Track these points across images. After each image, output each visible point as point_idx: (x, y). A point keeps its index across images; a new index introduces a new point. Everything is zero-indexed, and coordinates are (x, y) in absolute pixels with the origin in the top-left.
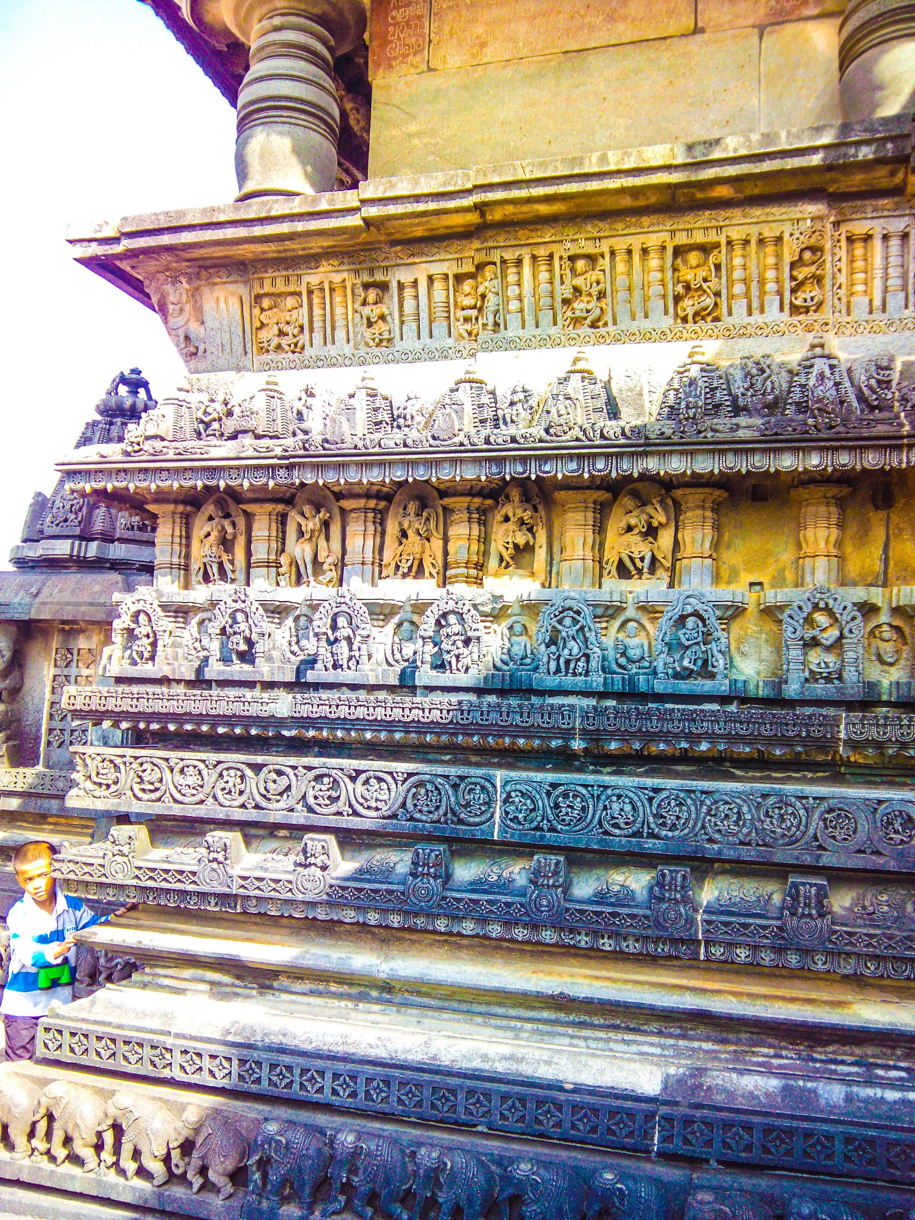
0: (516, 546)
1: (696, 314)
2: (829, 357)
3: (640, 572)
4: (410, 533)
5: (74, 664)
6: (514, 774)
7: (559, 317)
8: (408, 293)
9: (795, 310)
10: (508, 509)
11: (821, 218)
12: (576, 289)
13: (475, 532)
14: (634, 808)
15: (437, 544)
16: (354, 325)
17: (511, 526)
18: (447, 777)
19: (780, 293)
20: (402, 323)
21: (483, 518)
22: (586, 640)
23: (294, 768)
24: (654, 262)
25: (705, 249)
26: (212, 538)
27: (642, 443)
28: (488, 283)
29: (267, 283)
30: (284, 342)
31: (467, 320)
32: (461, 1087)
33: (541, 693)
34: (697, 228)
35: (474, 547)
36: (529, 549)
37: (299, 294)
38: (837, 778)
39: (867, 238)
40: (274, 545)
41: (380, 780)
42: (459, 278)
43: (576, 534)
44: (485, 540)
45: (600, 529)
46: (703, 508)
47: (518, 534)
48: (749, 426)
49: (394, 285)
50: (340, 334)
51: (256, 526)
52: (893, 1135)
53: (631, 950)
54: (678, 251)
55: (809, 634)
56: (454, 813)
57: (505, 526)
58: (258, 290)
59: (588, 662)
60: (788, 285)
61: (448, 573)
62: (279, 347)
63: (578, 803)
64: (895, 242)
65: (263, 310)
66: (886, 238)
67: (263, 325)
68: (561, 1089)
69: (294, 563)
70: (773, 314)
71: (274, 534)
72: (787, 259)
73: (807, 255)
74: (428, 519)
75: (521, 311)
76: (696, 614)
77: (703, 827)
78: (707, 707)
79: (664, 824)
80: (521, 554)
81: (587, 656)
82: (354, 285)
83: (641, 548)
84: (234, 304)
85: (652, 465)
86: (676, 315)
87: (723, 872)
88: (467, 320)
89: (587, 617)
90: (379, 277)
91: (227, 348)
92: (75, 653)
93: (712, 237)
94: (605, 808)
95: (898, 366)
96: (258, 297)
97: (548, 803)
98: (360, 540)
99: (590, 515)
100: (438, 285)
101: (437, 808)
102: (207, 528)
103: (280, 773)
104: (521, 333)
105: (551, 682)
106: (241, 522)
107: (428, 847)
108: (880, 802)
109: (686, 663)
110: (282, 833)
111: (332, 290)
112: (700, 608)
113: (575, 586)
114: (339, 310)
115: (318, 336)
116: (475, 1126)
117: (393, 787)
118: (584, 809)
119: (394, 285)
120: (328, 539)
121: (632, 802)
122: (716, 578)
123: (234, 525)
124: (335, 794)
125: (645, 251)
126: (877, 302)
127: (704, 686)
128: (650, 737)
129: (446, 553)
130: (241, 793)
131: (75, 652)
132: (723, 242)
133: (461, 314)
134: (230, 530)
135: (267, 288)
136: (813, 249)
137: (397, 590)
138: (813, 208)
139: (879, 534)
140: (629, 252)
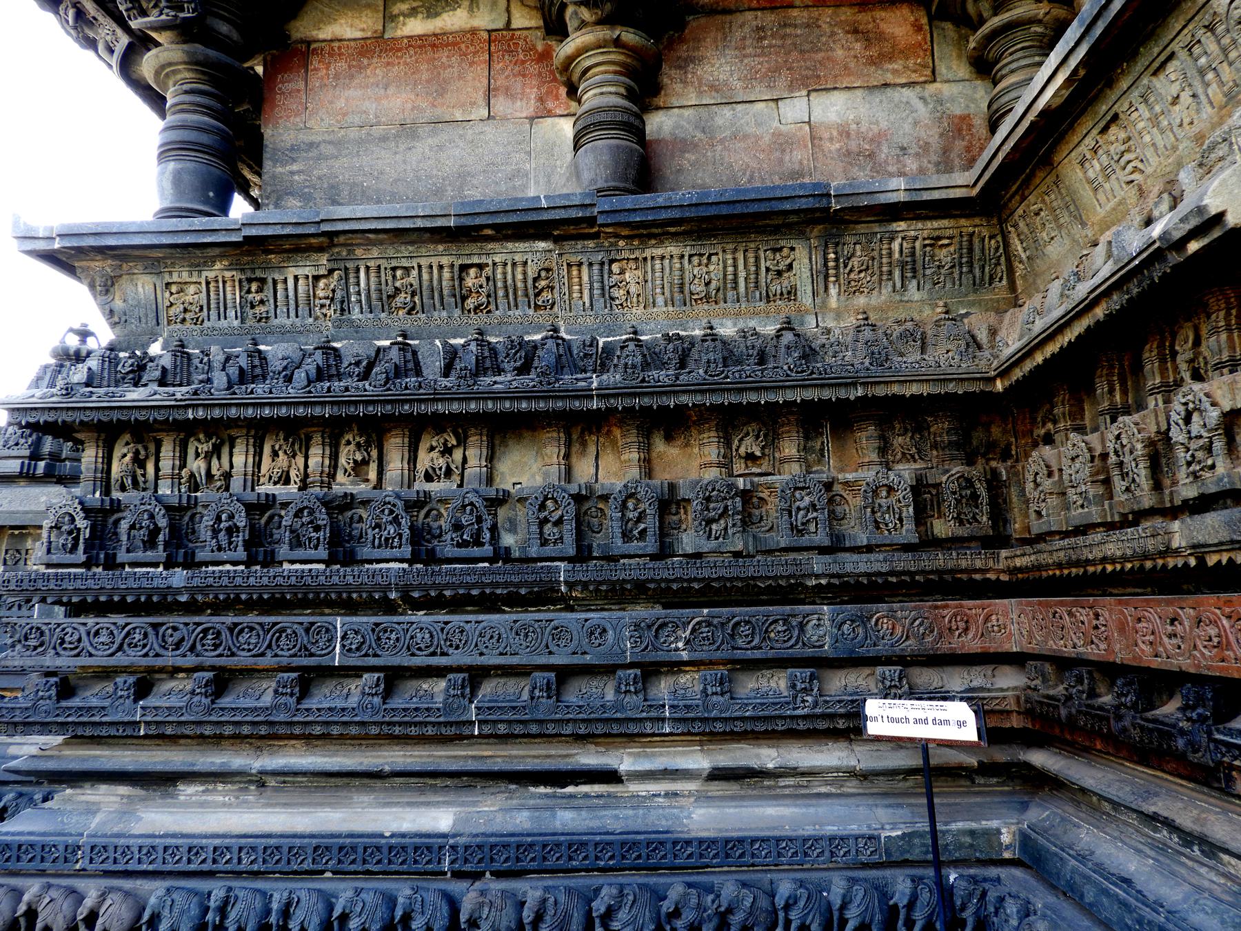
0: (355, 461)
1: (476, 308)
2: (558, 338)
3: (439, 477)
4: (280, 453)
5: (22, 562)
6: (348, 619)
7: (386, 307)
8: (280, 287)
9: (537, 307)
10: (349, 437)
11: (550, 251)
12: (396, 289)
13: (327, 452)
14: (432, 636)
15: (300, 460)
16: (241, 307)
17: (352, 447)
18: (301, 624)
19: (527, 295)
20: (276, 306)
22: (399, 524)
23: (186, 624)
24: (446, 274)
25: (481, 267)
26: (127, 459)
29: (175, 275)
30: (188, 316)
31: (322, 306)
32: (310, 844)
33: (370, 562)
35: (327, 462)
36: (365, 462)
37: (200, 283)
38: (571, 609)
39: (580, 264)
40: (177, 463)
41: (252, 629)
42: (317, 278)
44: (335, 457)
46: (481, 435)
47: (357, 454)
49: (270, 281)
50: (231, 313)
51: (163, 449)
52: (598, 838)
53: (430, 733)
54: (464, 268)
55: (542, 515)
56: (306, 649)
57: (348, 448)
58: (167, 279)
59: (400, 539)
60: (531, 292)
61: (309, 480)
62: (184, 320)
63: (393, 636)
64: (596, 268)
65: (172, 294)
66: (591, 265)
67: (172, 304)
68: (382, 836)
69: (192, 475)
71: (177, 454)
72: (531, 274)
73: (543, 274)
74: (293, 444)
75: (360, 301)
76: (472, 504)
77: (476, 645)
78: (481, 565)
79: (451, 646)
81: (400, 536)
82: (240, 281)
84: (149, 288)
85: (440, 407)
86: (463, 308)
87: (497, 676)
88: (322, 306)
89: (399, 509)
90: (259, 274)
91: (143, 320)
92: (23, 552)
93: (483, 260)
94: (412, 637)
95: (601, 344)
96: (168, 285)
97: (373, 638)
99: (406, 440)
100: (301, 282)
101: (294, 646)
102: (125, 450)
103: (175, 629)
104: (360, 316)
105: (377, 554)
106: (152, 448)
107: (286, 675)
108: (586, 620)
109: (465, 537)
110: (181, 675)
111: (224, 282)
112: (474, 500)
114: (229, 296)
115: (213, 313)
116: (322, 872)
117: (261, 633)
118: (398, 639)
119: (270, 281)
120: (219, 458)
121: (430, 632)
123: (146, 448)
124: (218, 642)
125: (441, 267)
126: (587, 304)
127: (476, 551)
128: (441, 587)
129: (306, 466)
130: (144, 646)
131: (23, 552)
132: (490, 263)
133: (317, 301)
134: (143, 452)
135: (175, 278)
136: (548, 270)
139: (592, 449)
140: (431, 267)
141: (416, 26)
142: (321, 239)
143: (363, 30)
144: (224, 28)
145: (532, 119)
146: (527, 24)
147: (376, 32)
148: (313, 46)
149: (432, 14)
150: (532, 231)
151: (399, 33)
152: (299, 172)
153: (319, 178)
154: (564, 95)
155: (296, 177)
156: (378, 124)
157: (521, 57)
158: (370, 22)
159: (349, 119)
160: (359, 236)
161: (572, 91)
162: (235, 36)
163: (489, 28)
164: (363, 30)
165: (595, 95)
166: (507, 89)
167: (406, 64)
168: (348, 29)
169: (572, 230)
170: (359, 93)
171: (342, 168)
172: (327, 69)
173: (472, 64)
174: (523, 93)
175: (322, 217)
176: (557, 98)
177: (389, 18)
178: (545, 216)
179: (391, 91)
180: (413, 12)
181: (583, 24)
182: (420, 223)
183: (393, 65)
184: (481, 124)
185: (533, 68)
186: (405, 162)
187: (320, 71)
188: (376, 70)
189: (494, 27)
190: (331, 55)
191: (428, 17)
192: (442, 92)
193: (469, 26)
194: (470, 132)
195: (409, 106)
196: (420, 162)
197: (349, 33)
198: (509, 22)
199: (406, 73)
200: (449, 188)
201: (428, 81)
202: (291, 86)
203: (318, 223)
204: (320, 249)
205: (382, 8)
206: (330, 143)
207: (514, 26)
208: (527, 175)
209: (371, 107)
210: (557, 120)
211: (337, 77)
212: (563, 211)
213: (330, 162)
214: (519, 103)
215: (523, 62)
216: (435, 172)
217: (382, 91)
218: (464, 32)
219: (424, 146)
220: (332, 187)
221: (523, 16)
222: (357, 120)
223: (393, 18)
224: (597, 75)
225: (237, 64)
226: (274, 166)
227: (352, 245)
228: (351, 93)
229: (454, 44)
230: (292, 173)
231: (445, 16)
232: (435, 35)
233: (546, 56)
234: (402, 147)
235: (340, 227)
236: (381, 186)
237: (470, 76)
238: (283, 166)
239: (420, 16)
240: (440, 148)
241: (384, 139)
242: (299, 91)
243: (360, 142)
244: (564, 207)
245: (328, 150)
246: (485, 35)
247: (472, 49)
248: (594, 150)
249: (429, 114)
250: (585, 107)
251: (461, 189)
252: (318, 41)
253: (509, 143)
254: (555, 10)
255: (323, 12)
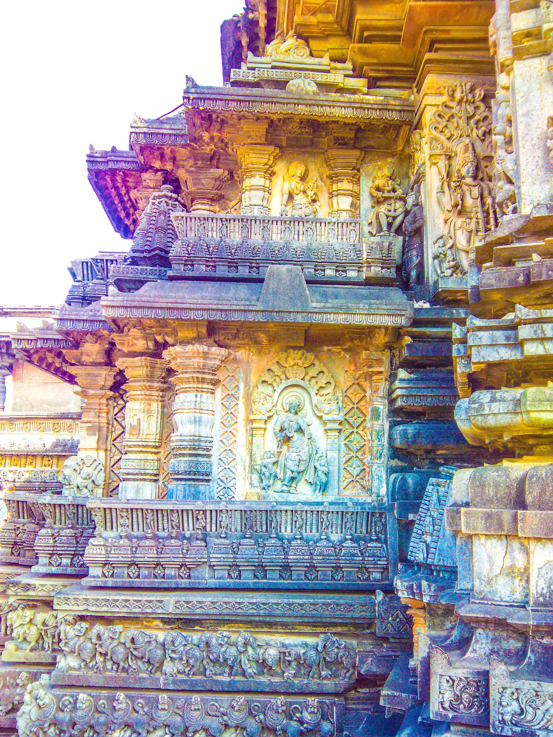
21: (26, 458)
27: (46, 451)
28: (28, 425)
34: (56, 421)
43: (39, 460)
45: (43, 460)
48: (60, 449)
70: (66, 432)
80: (31, 463)
83: (47, 463)
98: (8, 461)
113: (38, 468)
122: (57, 467)
137: (13, 468)
138: (71, 420)
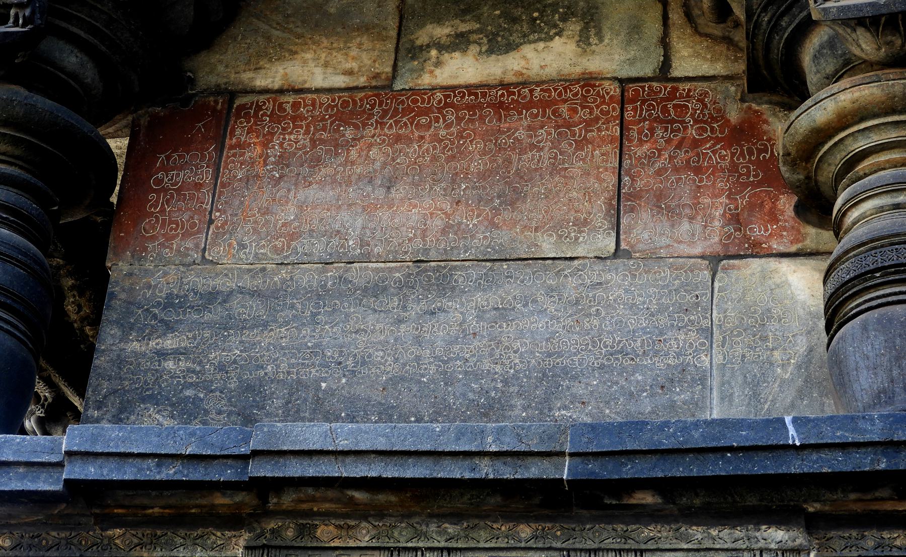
141: (464, 68)
142: (239, 497)
143: (350, 73)
144: (71, 58)
145: (715, 260)
146: (705, 69)
147: (377, 76)
148: (238, 102)
149: (498, 45)
150: (752, 501)
151: (426, 80)
152: (177, 353)
153: (221, 368)
154: (789, 212)
155: (170, 365)
156: (366, 258)
157: (692, 132)
158: (366, 59)
159: (302, 245)
160: (330, 494)
161: (816, 206)
162: (90, 74)
163: (624, 73)
164: (350, 73)
165: (881, 209)
166: (660, 196)
167: (436, 139)
168: (318, 71)
169: (852, 502)
170: (330, 194)
171: (275, 348)
172: (265, 145)
173: (580, 144)
174: (696, 205)
175: (253, 445)
176: (773, 217)
177: (407, 51)
178: (796, 466)
179: (398, 193)
180: (460, 42)
181: (849, 66)
182: (486, 470)
183: (409, 141)
184: (598, 266)
185: (722, 157)
186: (418, 341)
187: (248, 149)
188: (371, 151)
189: (634, 73)
190: (276, 118)
191: (490, 51)
192: (513, 198)
193: (578, 70)
194: (572, 282)
195: (438, 223)
196: (455, 341)
197: (319, 78)
198: (666, 64)
199: (434, 159)
200: (519, 402)
201: (483, 176)
202: (184, 176)
203: (244, 458)
204: (233, 521)
205: (393, 33)
206: (254, 293)
207: (676, 73)
208: (703, 380)
209: (353, 223)
210: (772, 263)
211: (283, 160)
212: (840, 456)
213: (249, 336)
214: (685, 226)
215: (696, 144)
216: (486, 365)
217: (380, 193)
218: (567, 82)
219: (462, 310)
220: (248, 388)
221: (697, 55)
222: (319, 248)
223: (416, 52)
224: (880, 171)
225: (87, 126)
226: (124, 339)
227: (310, 514)
228: (312, 193)
229: (544, 104)
230: (162, 354)
231: (528, 50)
232: (503, 85)
233: (746, 133)
234: (415, 309)
235: (295, 469)
236: (360, 390)
237: (576, 169)
238: (144, 337)
239: (474, 49)
240: (503, 313)
241: (376, 290)
242: (198, 186)
243: (320, 295)
244: (843, 446)
245: (242, 308)
246: (614, 89)
247: (583, 114)
248: (884, 325)
249: (479, 243)
250: (848, 240)
251: (546, 404)
252: (253, 91)
253: (662, 309)
254: (779, 42)
255: (268, 38)
